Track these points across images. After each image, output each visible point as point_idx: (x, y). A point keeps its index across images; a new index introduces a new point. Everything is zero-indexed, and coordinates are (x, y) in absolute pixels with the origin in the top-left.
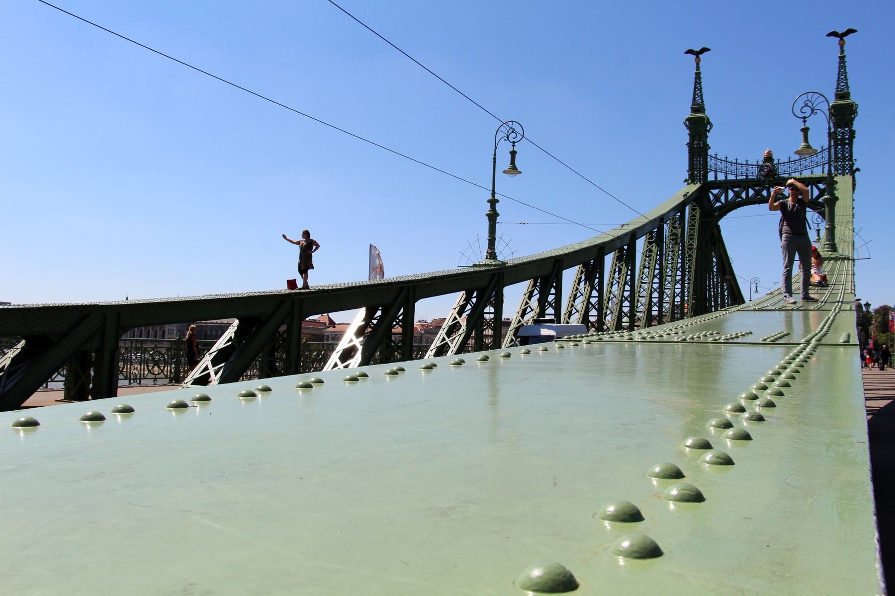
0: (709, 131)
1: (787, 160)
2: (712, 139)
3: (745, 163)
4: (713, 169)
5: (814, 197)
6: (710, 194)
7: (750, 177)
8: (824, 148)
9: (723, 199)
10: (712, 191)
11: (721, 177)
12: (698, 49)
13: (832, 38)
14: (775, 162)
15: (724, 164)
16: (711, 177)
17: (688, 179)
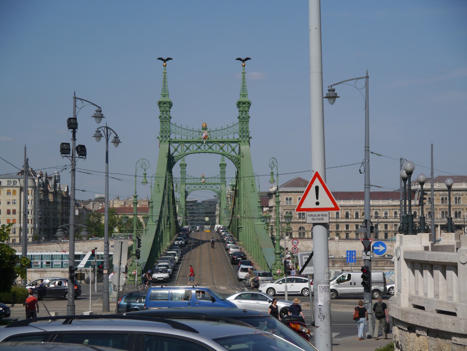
0: (170, 108)
1: (215, 130)
2: (173, 112)
3: (192, 129)
4: (174, 132)
5: (229, 152)
6: (170, 145)
7: (195, 138)
8: (234, 124)
9: (179, 149)
10: (173, 144)
11: (178, 138)
12: (165, 58)
13: (239, 61)
14: (209, 130)
15: (180, 129)
16: (172, 137)
17: (160, 136)
